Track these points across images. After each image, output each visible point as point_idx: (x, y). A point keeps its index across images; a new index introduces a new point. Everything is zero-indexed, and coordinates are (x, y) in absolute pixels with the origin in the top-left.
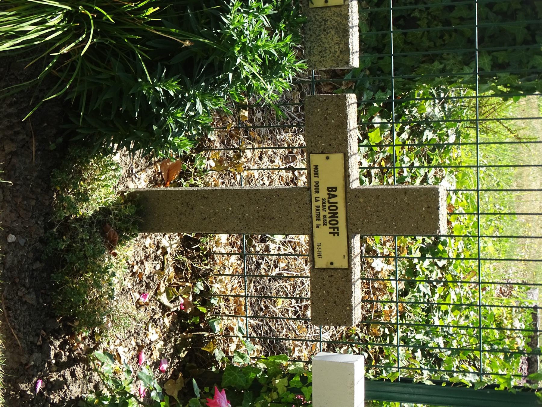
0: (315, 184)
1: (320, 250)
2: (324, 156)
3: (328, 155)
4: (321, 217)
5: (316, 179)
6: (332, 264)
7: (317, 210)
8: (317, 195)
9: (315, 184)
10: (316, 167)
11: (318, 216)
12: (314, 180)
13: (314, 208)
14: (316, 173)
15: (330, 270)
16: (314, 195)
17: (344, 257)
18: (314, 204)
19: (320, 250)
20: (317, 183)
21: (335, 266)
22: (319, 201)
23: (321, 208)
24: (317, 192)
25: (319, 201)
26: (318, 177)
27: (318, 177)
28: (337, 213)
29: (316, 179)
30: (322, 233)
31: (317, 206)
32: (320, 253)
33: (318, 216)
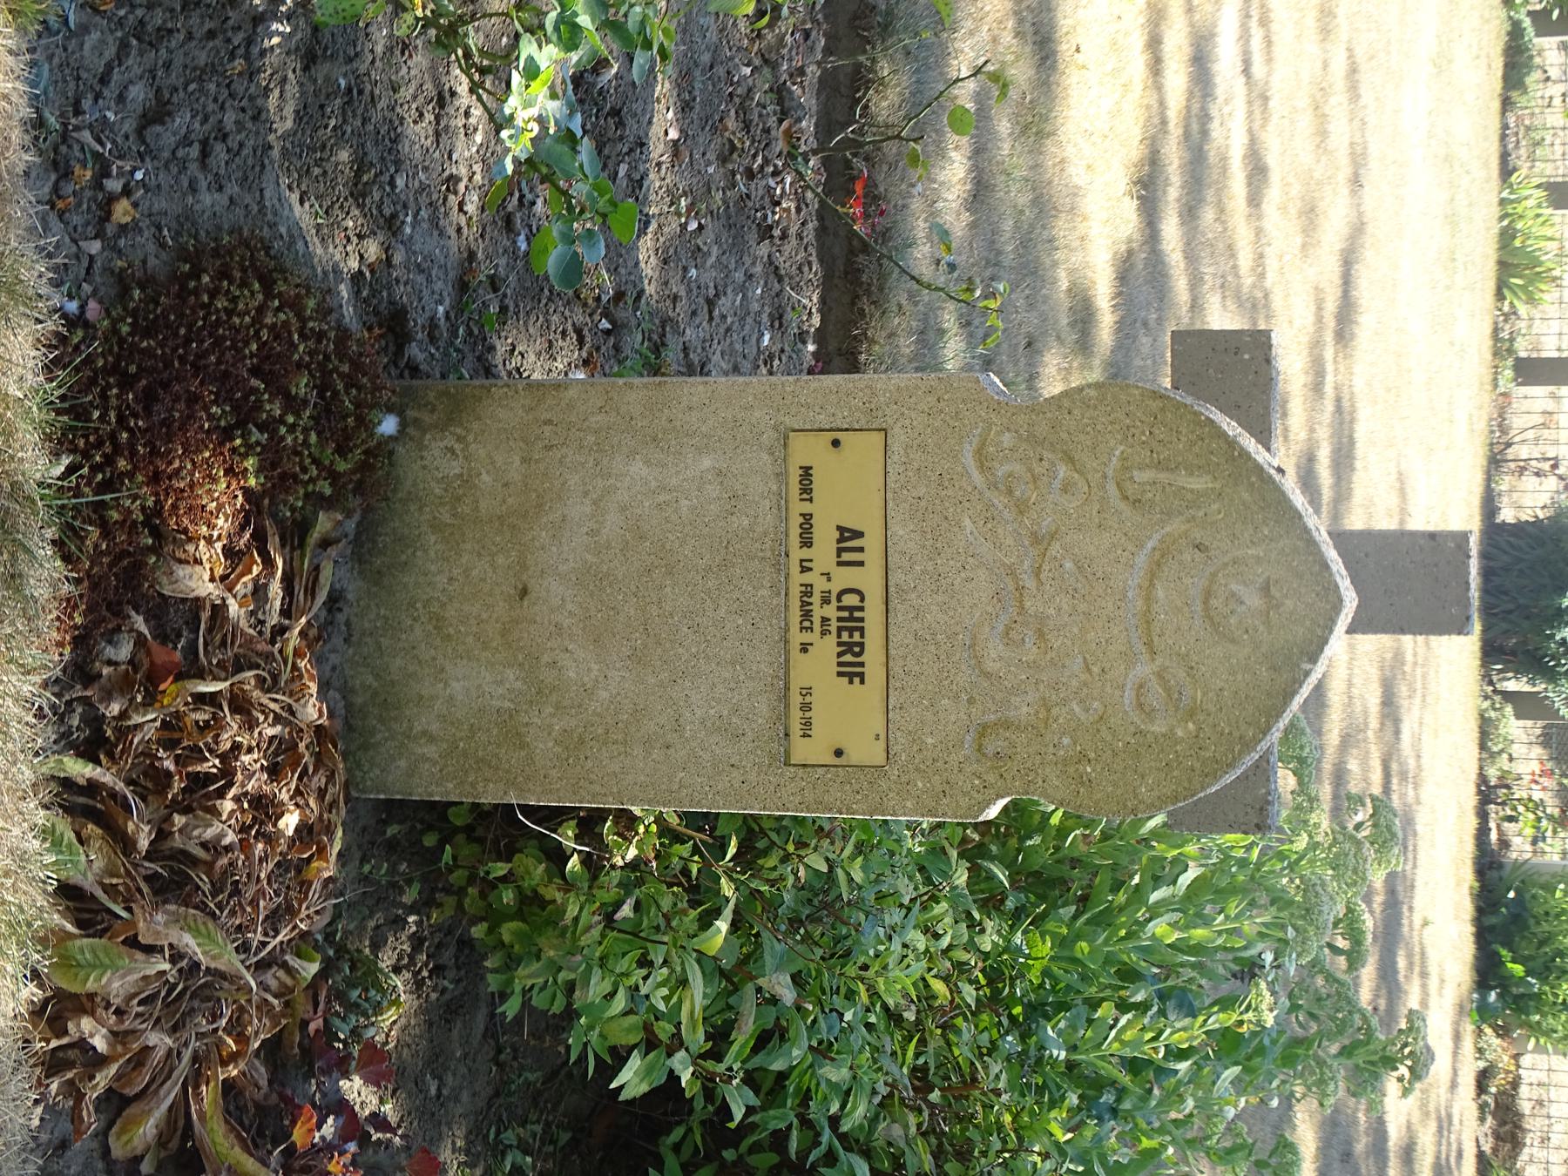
0: (801, 520)
1: (807, 715)
5: (806, 507)
8: (805, 553)
9: (801, 520)
10: (806, 471)
11: (807, 615)
12: (797, 507)
14: (806, 490)
16: (797, 553)
17: (877, 737)
18: (797, 578)
19: (807, 715)
20: (807, 518)
24: (807, 543)
26: (811, 500)
27: (811, 500)
29: (806, 507)
32: (807, 724)
33: (807, 615)
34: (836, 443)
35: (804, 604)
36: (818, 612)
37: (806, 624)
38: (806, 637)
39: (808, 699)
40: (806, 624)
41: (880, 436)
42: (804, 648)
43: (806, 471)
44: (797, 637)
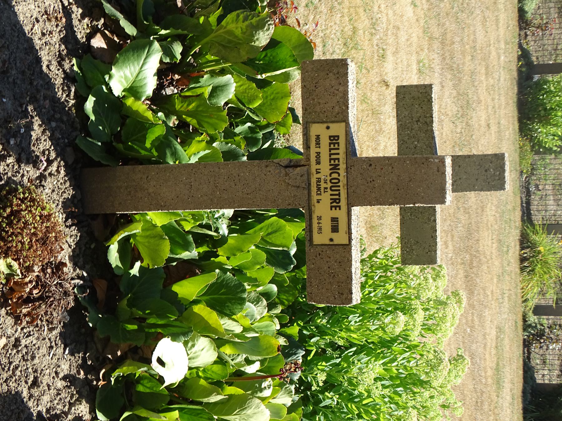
0: (316, 155)
1: (320, 225)
2: (326, 125)
3: (331, 125)
4: (322, 190)
5: (318, 150)
6: (331, 240)
7: (318, 181)
8: (318, 167)
9: (316, 155)
10: (318, 137)
11: (319, 189)
12: (313, 150)
13: (314, 181)
14: (318, 144)
15: (332, 246)
16: (314, 167)
20: (318, 154)
21: (335, 242)
22: (320, 172)
23: (322, 181)
24: (318, 163)
25: (320, 172)
26: (320, 147)
27: (320, 147)
28: (339, 165)
29: (318, 150)
30: (322, 209)
31: (318, 178)
32: (320, 229)
33: (319, 189)
34: (328, 128)
35: (318, 185)
36: (323, 185)
37: (319, 192)
38: (319, 197)
39: (320, 221)
40: (319, 192)
41: (344, 123)
42: (318, 201)
43: (318, 137)
44: (315, 197)
